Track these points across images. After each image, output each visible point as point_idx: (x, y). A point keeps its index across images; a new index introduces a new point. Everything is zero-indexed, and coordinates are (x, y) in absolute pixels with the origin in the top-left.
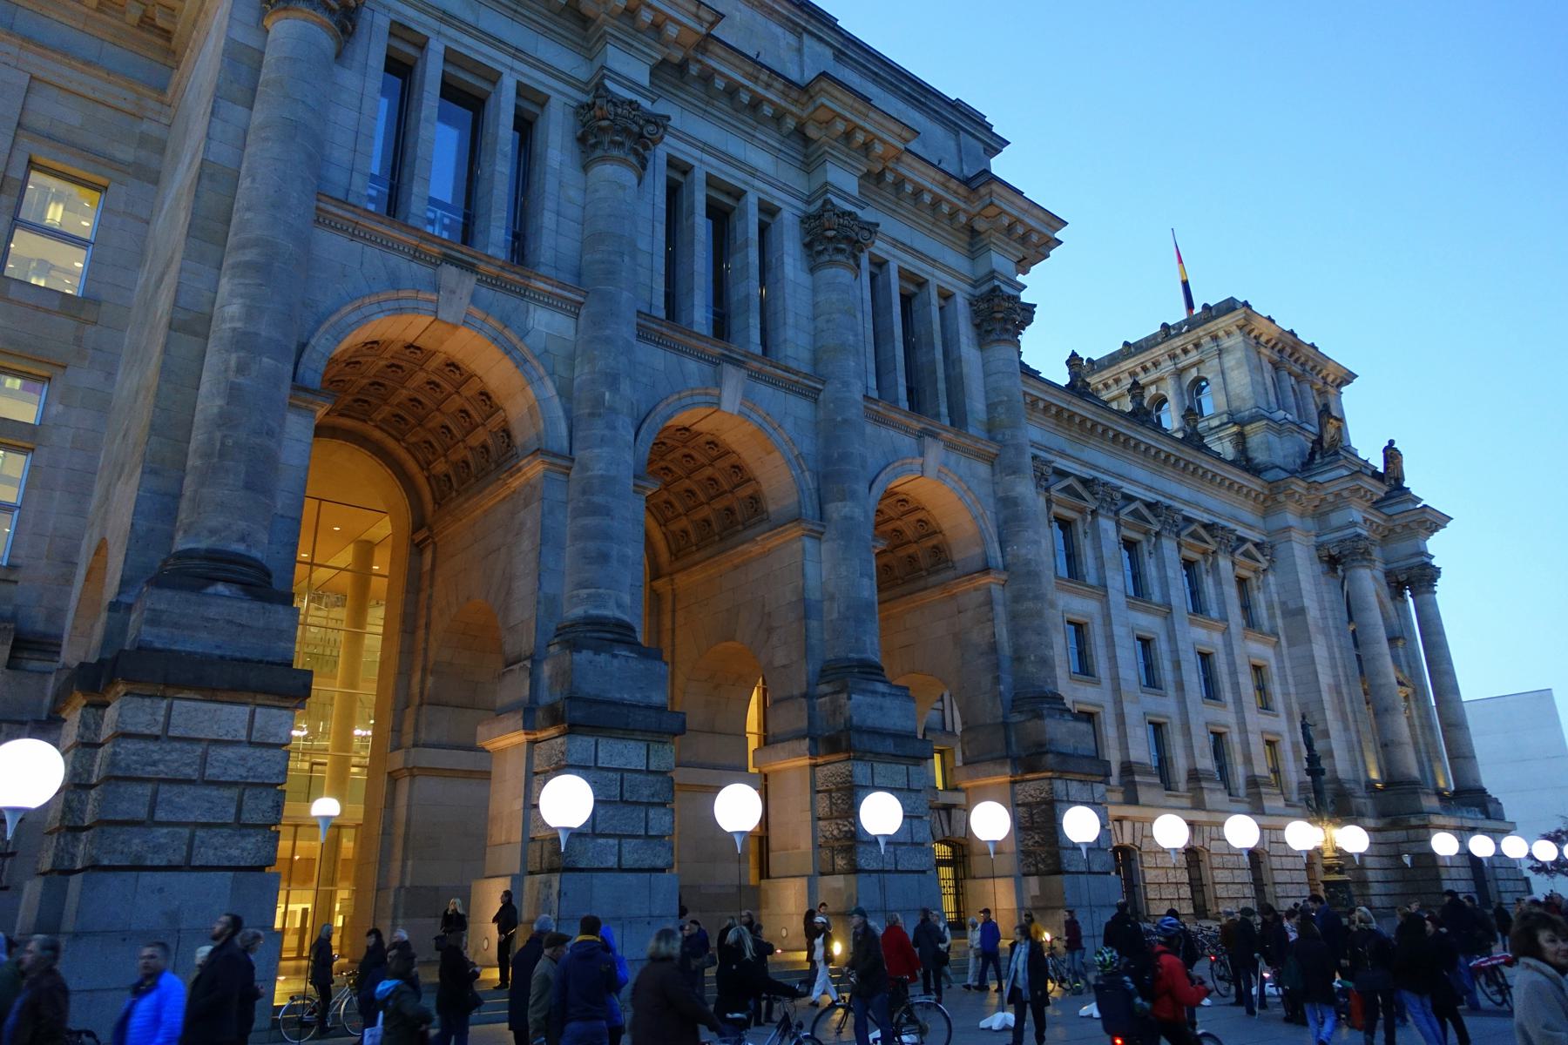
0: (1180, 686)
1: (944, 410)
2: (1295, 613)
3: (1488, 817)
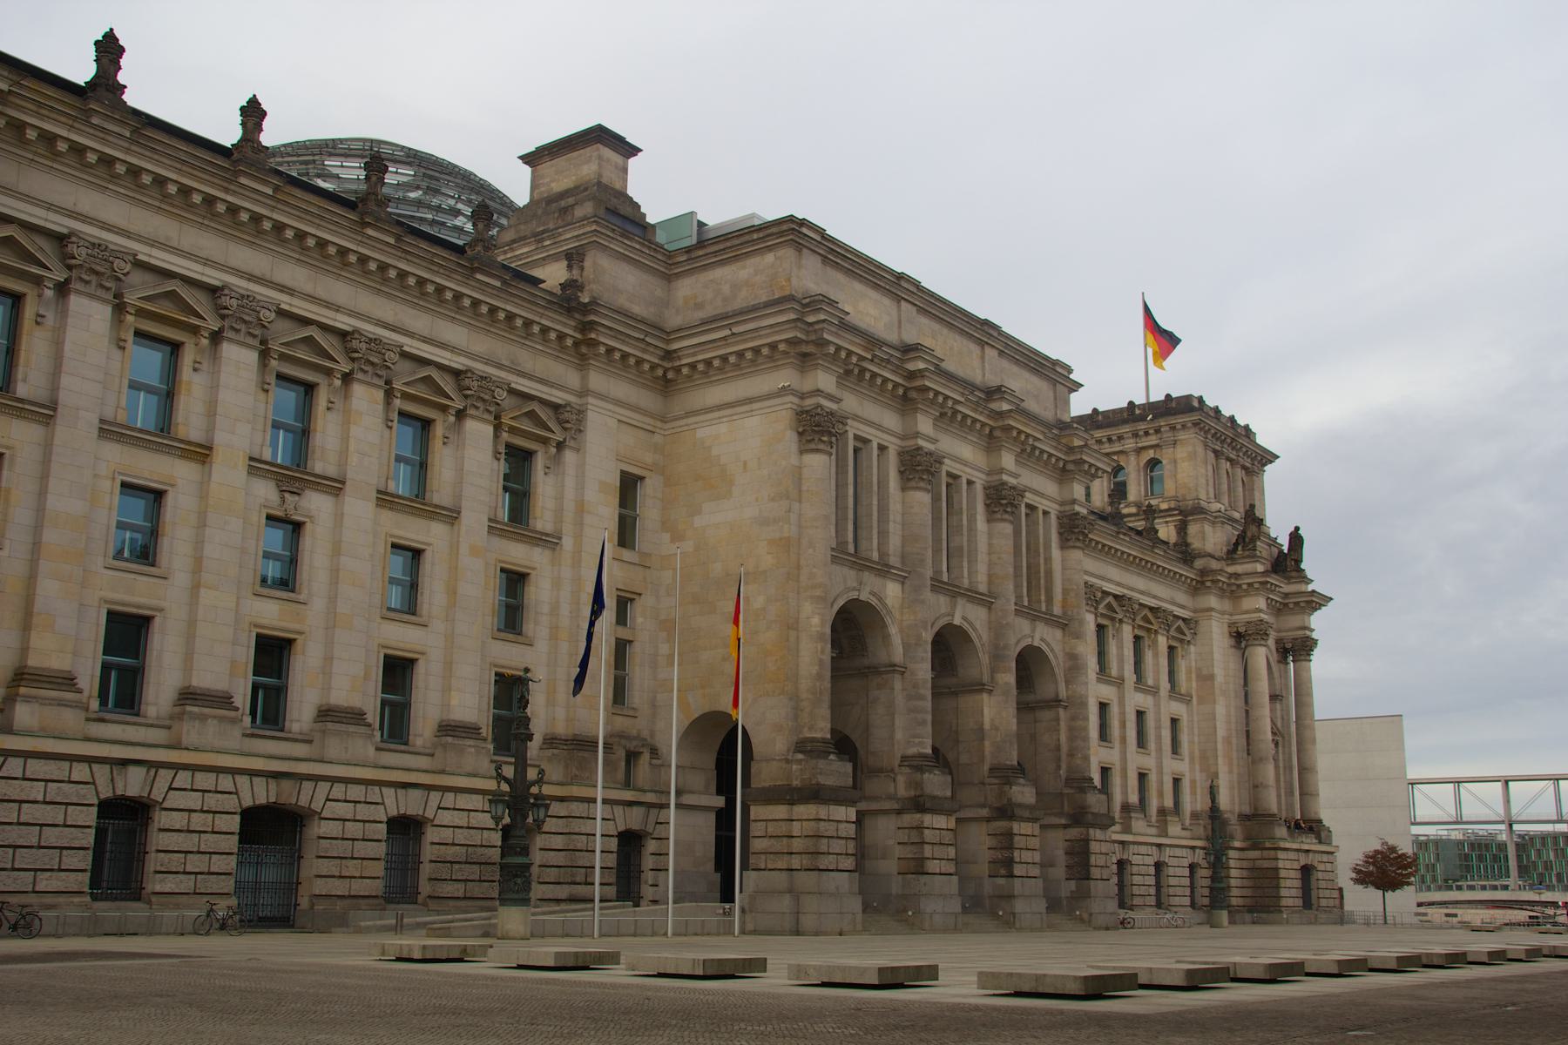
0: (1123, 740)
1: (1043, 598)
2: (1206, 678)
3: (1320, 842)
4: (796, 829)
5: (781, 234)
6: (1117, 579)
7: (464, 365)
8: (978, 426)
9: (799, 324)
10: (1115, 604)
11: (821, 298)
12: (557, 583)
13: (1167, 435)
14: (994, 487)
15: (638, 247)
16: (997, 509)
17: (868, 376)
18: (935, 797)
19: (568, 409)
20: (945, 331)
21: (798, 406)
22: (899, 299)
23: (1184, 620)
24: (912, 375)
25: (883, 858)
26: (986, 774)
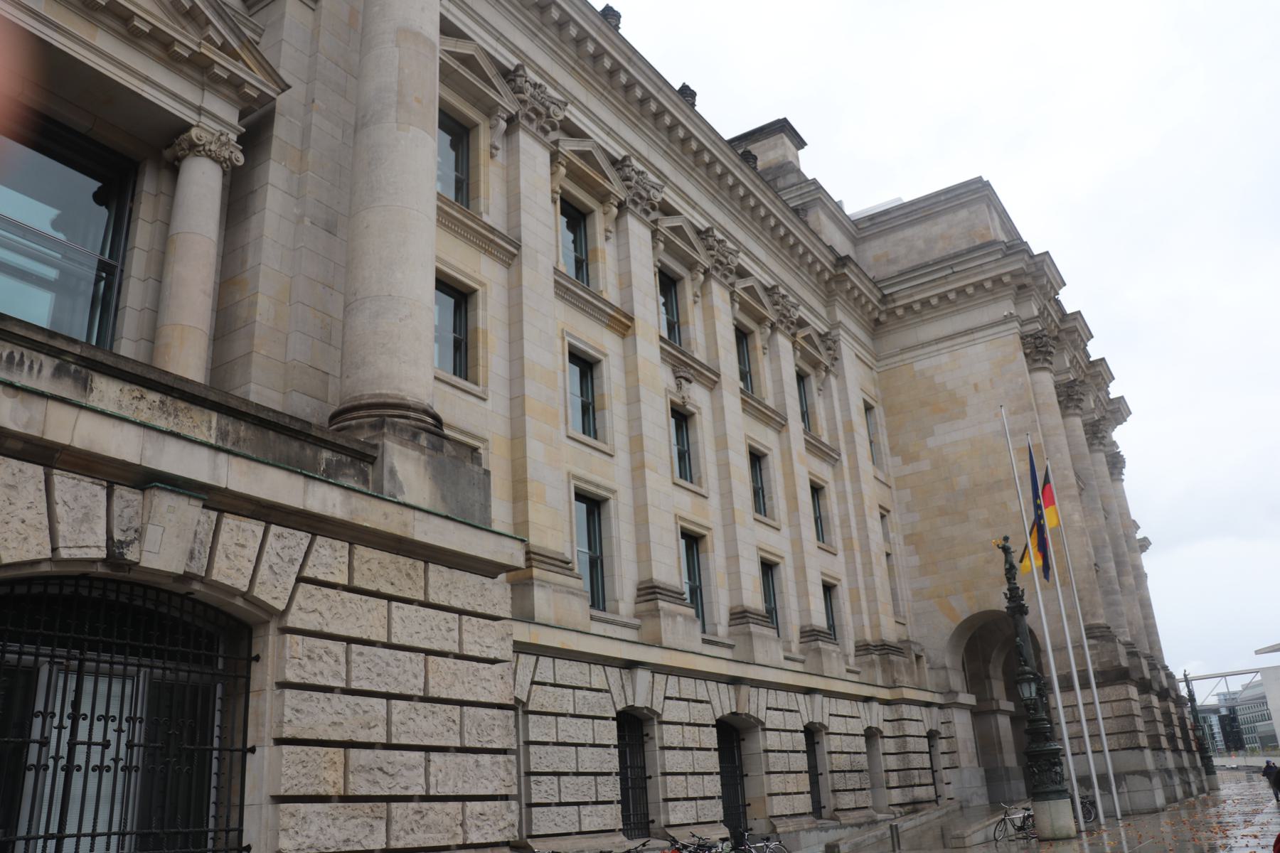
7: (768, 283)
12: (842, 497)
14: (1090, 424)
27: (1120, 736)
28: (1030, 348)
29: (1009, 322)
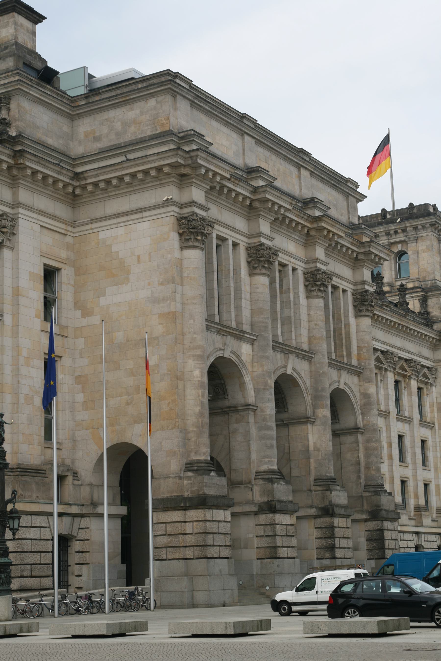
0: (390, 457)
1: (345, 353)
4: (189, 528)
5: (161, 84)
6: (382, 339)
8: (300, 227)
9: (180, 152)
10: (382, 357)
11: (193, 132)
13: (411, 232)
15: (49, 93)
16: (313, 289)
17: (226, 191)
18: (282, 502)
19: (5, 217)
20: (274, 157)
21: (178, 213)
22: (242, 133)
23: (428, 368)
24: (255, 190)
25: (246, 547)
26: (312, 483)
27: (195, 548)
28: (182, 229)
29: (168, 206)
